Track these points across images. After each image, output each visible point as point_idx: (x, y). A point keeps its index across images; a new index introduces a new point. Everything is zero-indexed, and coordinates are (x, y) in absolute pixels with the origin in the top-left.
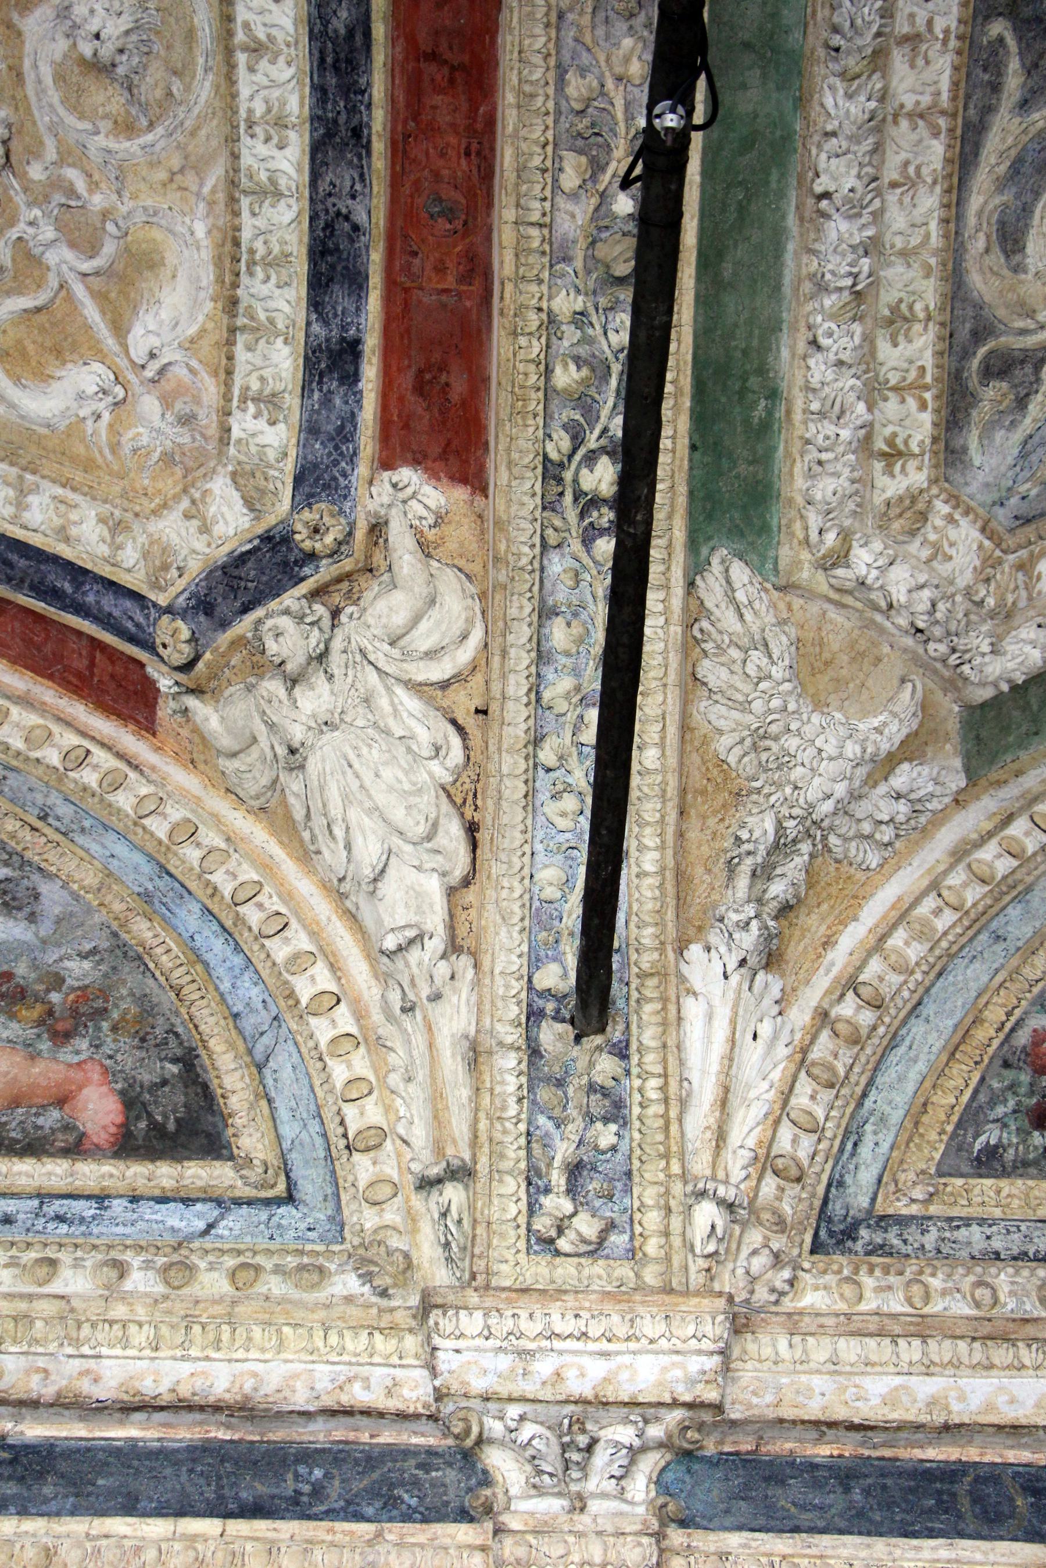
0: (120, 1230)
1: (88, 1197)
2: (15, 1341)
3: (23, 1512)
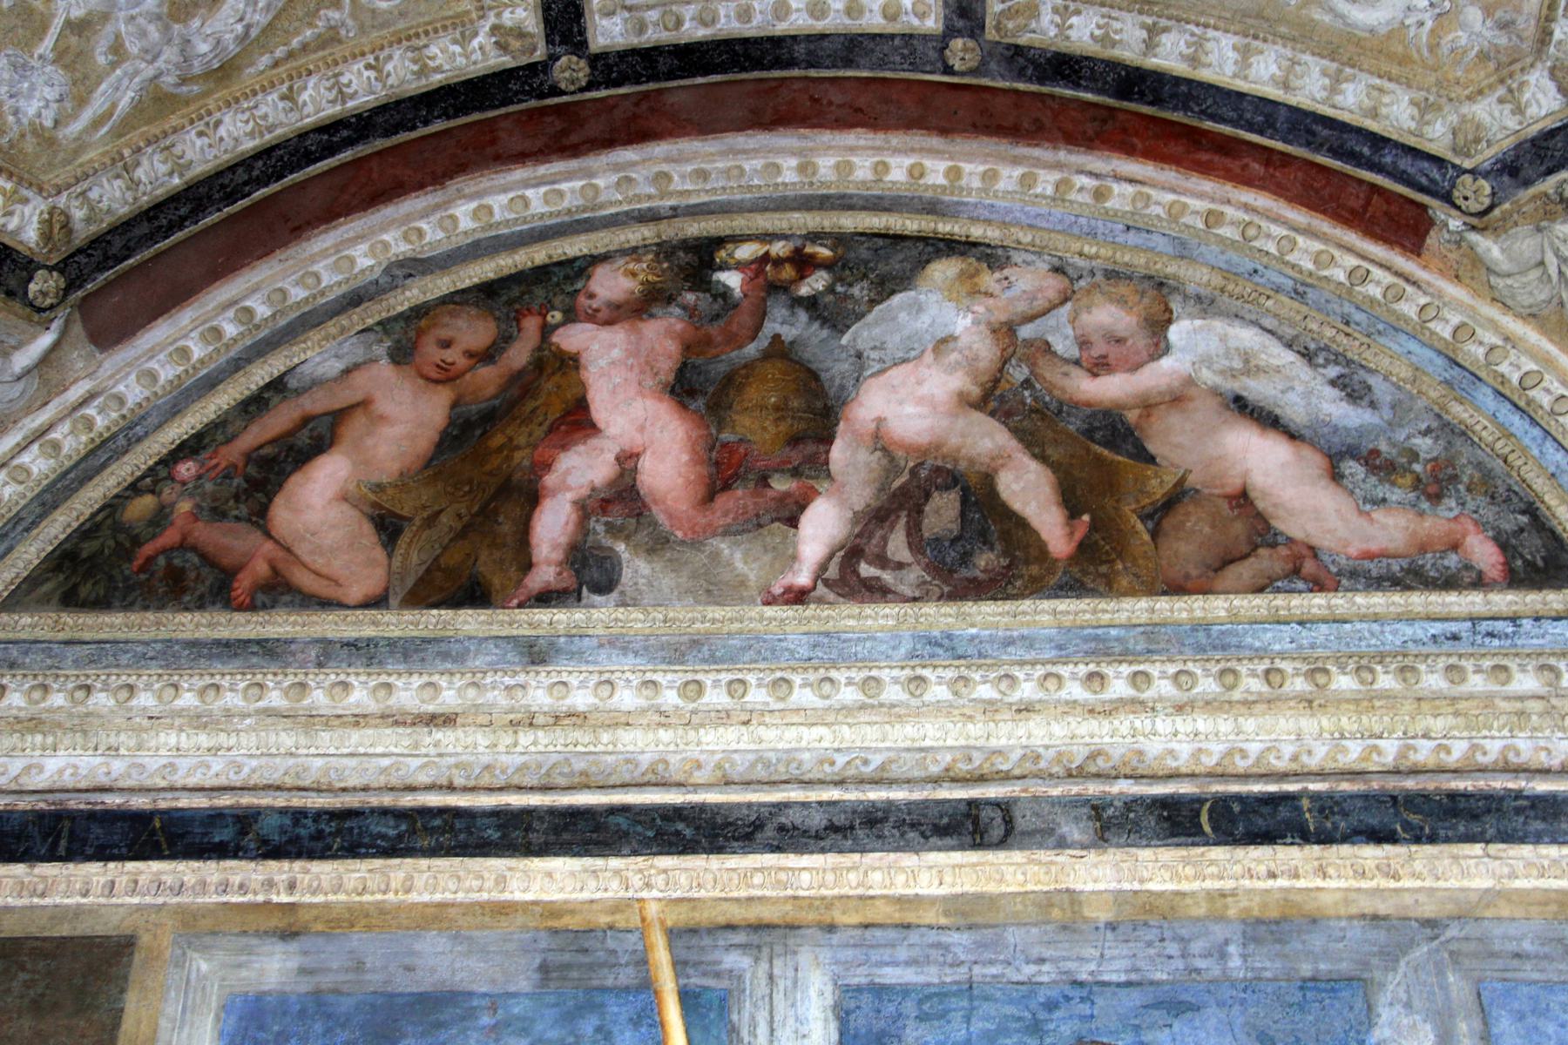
0: (1535, 641)
1: (1505, 619)
2: (1521, 730)
3: (1554, 841)
